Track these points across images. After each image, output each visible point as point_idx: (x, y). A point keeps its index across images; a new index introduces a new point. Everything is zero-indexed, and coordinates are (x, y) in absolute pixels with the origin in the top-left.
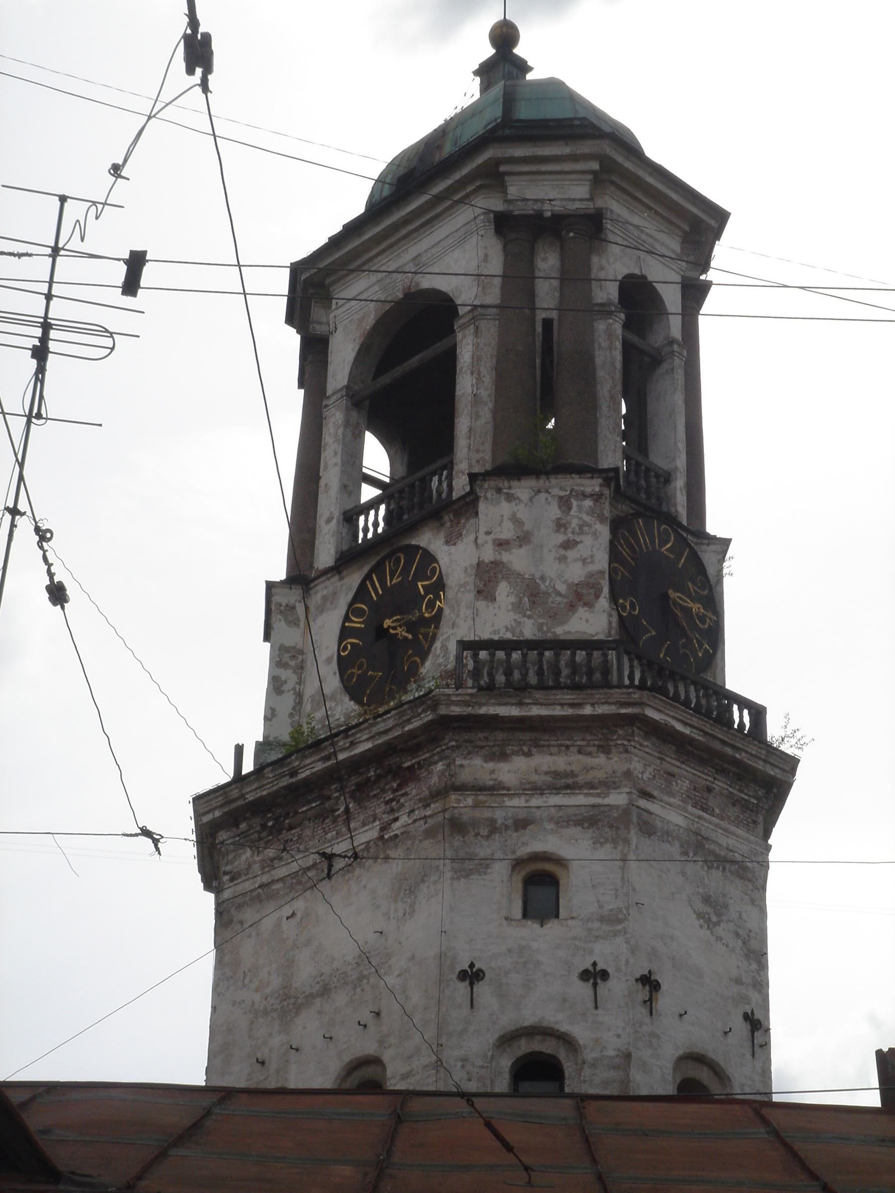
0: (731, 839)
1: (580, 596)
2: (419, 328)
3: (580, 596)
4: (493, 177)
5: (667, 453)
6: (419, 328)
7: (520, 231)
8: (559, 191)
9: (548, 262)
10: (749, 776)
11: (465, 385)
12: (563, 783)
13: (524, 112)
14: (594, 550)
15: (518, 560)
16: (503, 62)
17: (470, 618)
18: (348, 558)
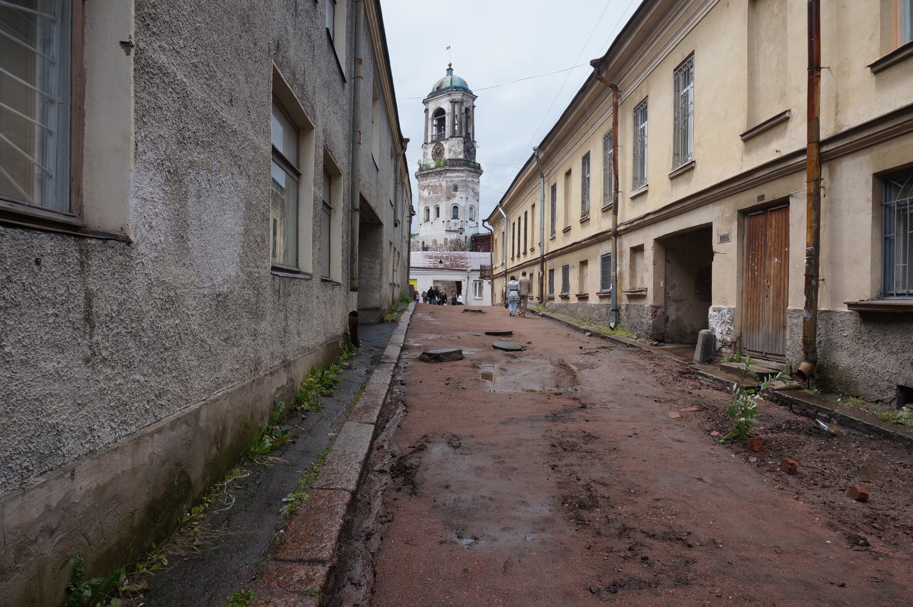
0: (476, 180)
1: (460, 153)
2: (440, 112)
3: (460, 153)
4: (450, 95)
5: (470, 131)
6: (440, 112)
7: (453, 102)
8: (458, 96)
9: (457, 107)
10: (477, 170)
11: (447, 123)
12: (458, 177)
13: (454, 84)
14: (462, 147)
15: (453, 148)
16: (450, 70)
17: (447, 156)
18: (432, 142)
